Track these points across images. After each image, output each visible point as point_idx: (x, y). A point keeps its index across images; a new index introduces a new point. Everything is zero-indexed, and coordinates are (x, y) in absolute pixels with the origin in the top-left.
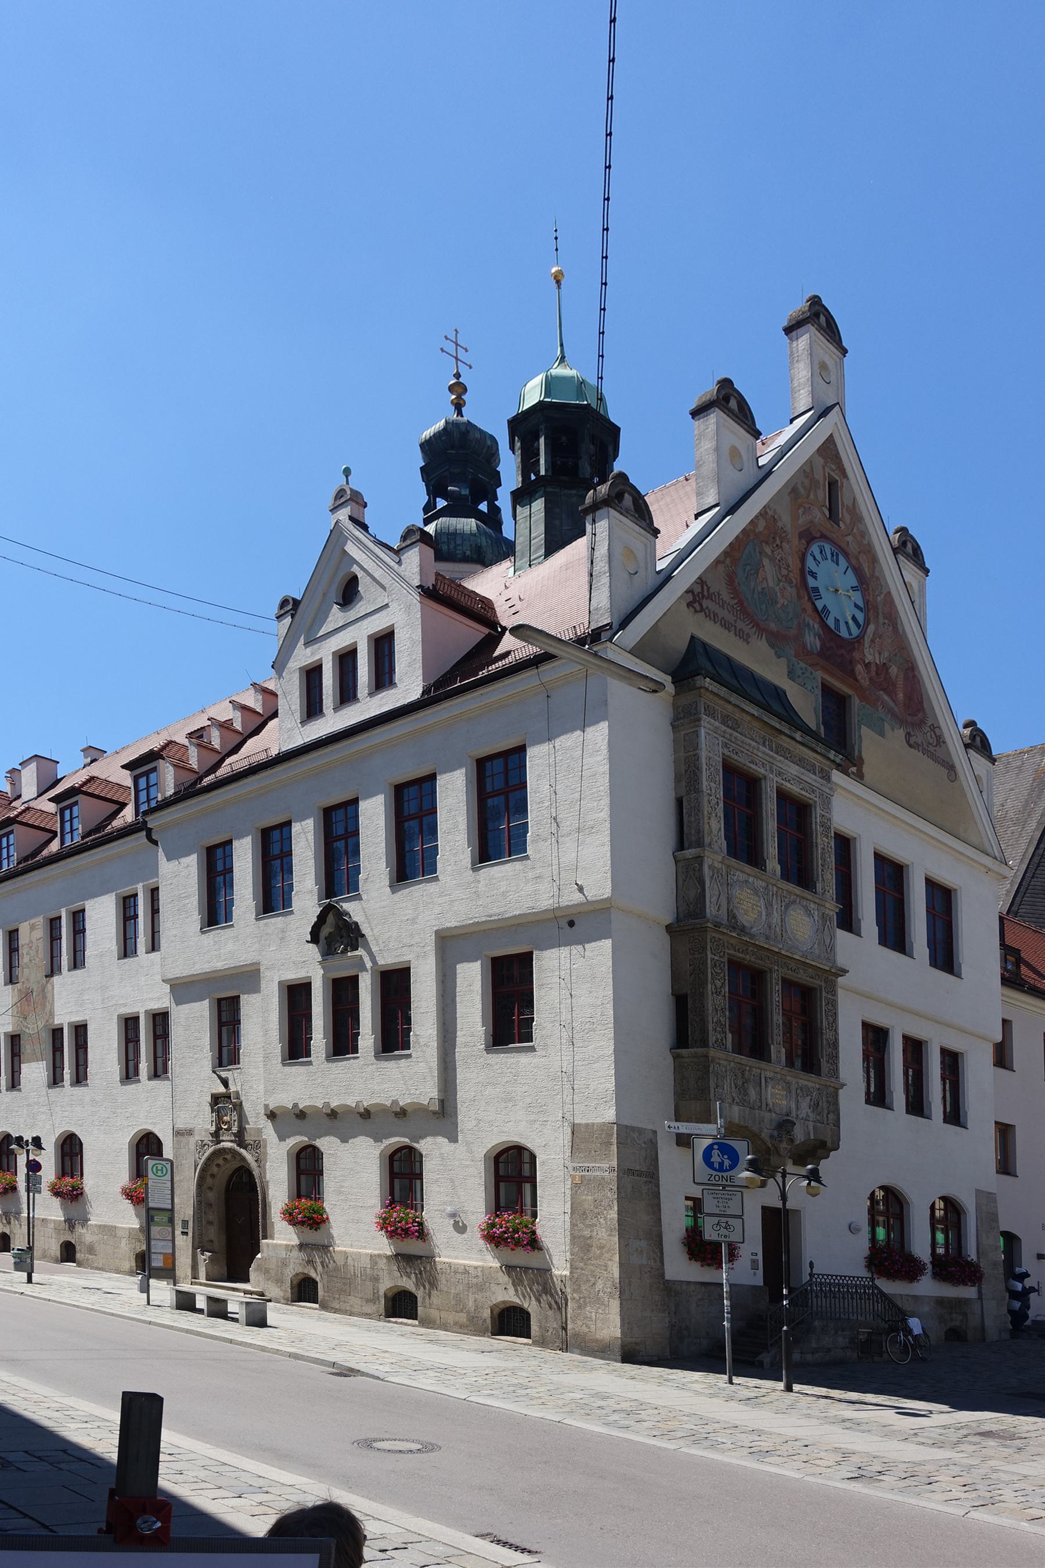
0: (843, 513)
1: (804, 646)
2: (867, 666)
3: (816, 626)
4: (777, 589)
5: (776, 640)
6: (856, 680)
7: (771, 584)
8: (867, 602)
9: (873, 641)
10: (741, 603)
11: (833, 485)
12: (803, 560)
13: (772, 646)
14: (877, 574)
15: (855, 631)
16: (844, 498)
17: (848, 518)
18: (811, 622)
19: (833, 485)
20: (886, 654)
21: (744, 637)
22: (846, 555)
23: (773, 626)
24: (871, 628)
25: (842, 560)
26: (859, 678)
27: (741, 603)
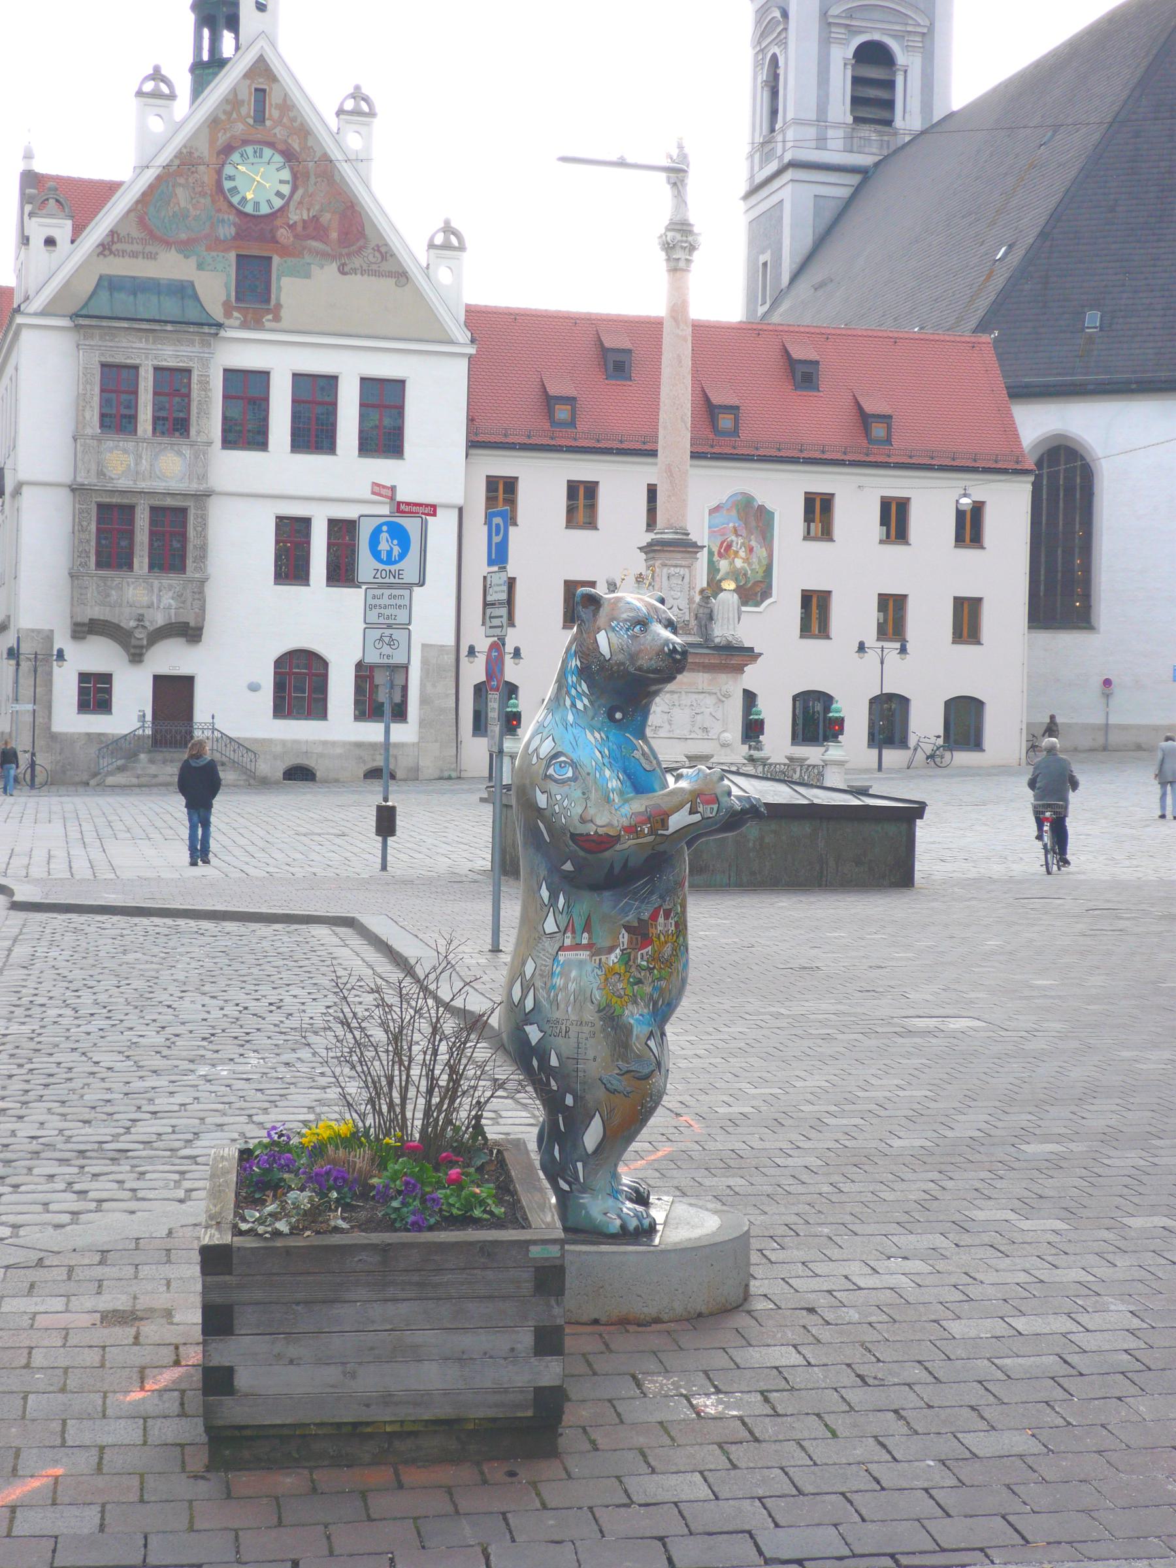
0: (273, 113)
1: (217, 239)
2: (292, 227)
3: (231, 217)
4: (190, 207)
5: (185, 247)
6: (277, 242)
7: (183, 204)
8: (295, 176)
9: (300, 203)
10: (151, 233)
11: (261, 92)
12: (219, 172)
13: (179, 251)
14: (310, 144)
15: (278, 203)
16: (274, 98)
17: (276, 114)
18: (226, 217)
19: (261, 92)
20: (317, 207)
21: (152, 256)
22: (271, 145)
23: (183, 236)
24: (300, 192)
25: (268, 152)
26: (282, 240)
27: (151, 233)
